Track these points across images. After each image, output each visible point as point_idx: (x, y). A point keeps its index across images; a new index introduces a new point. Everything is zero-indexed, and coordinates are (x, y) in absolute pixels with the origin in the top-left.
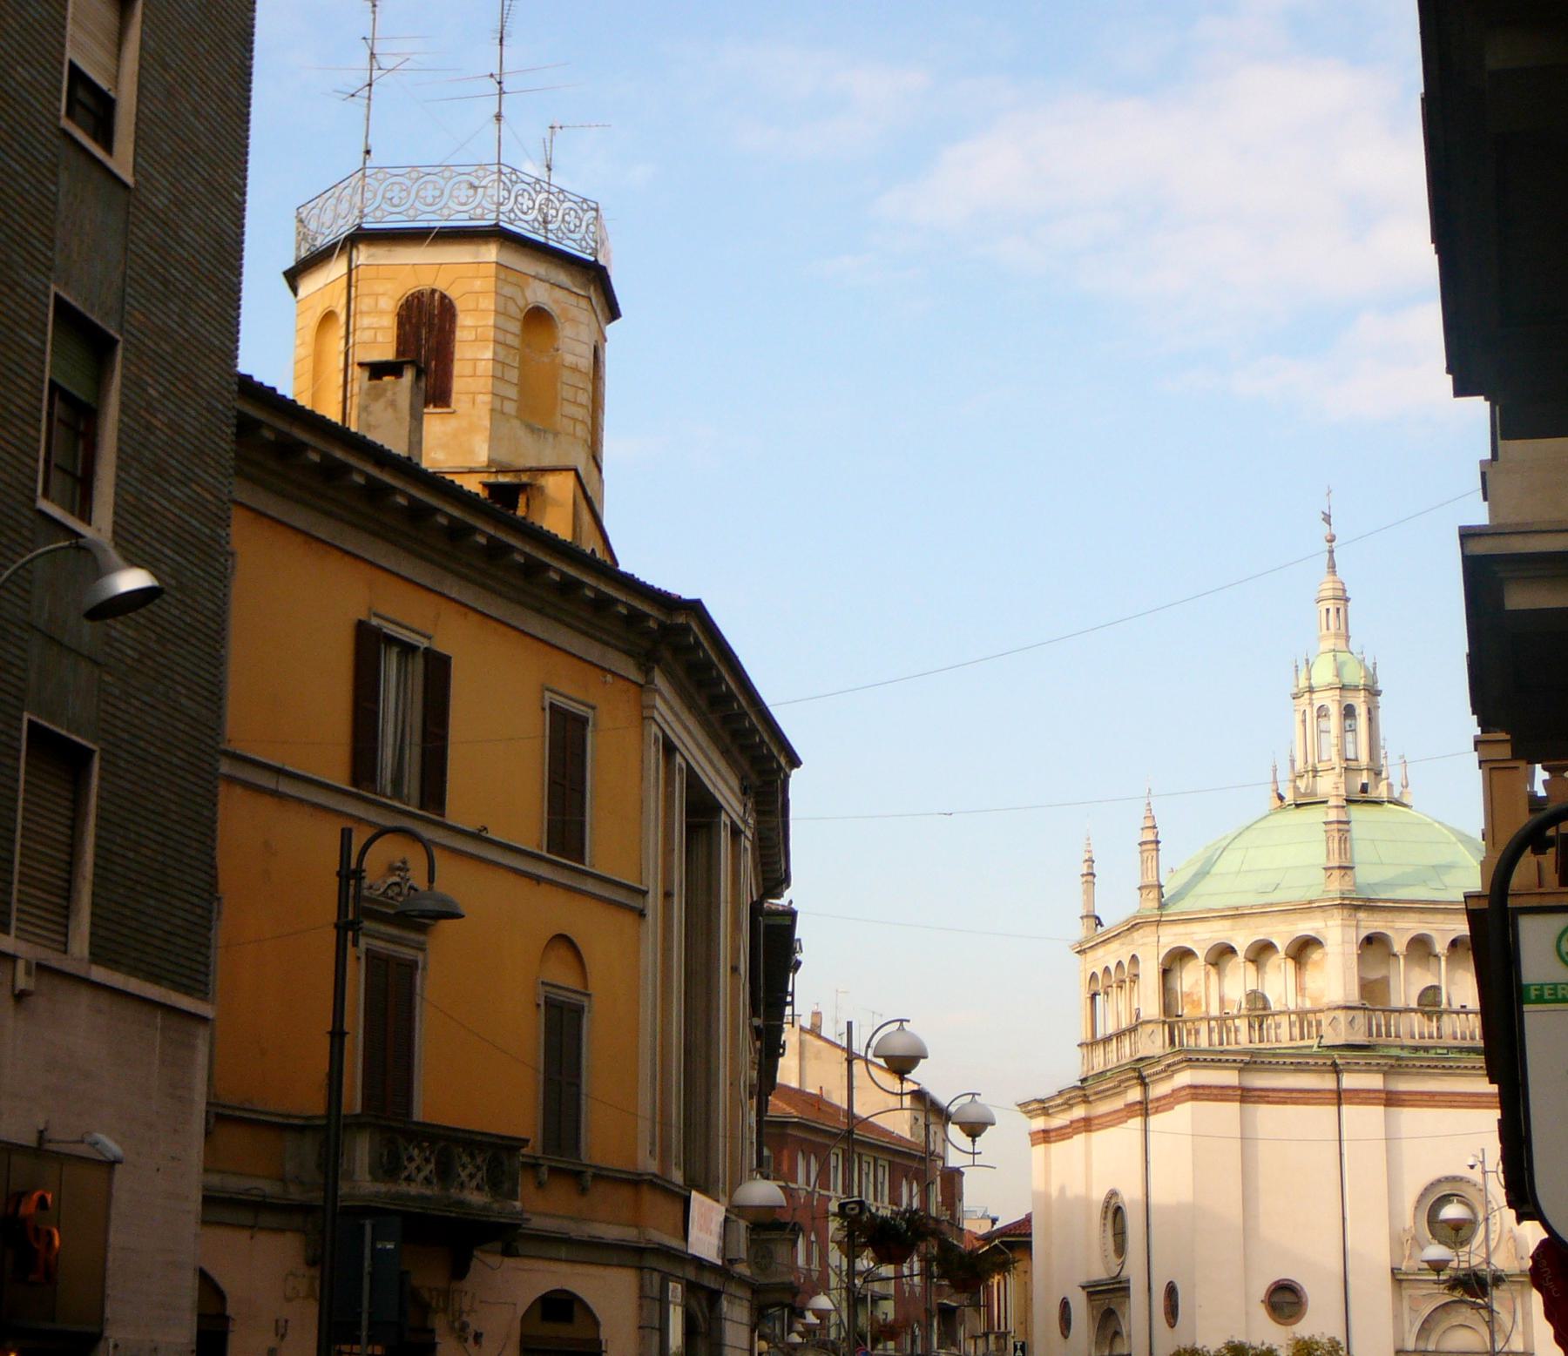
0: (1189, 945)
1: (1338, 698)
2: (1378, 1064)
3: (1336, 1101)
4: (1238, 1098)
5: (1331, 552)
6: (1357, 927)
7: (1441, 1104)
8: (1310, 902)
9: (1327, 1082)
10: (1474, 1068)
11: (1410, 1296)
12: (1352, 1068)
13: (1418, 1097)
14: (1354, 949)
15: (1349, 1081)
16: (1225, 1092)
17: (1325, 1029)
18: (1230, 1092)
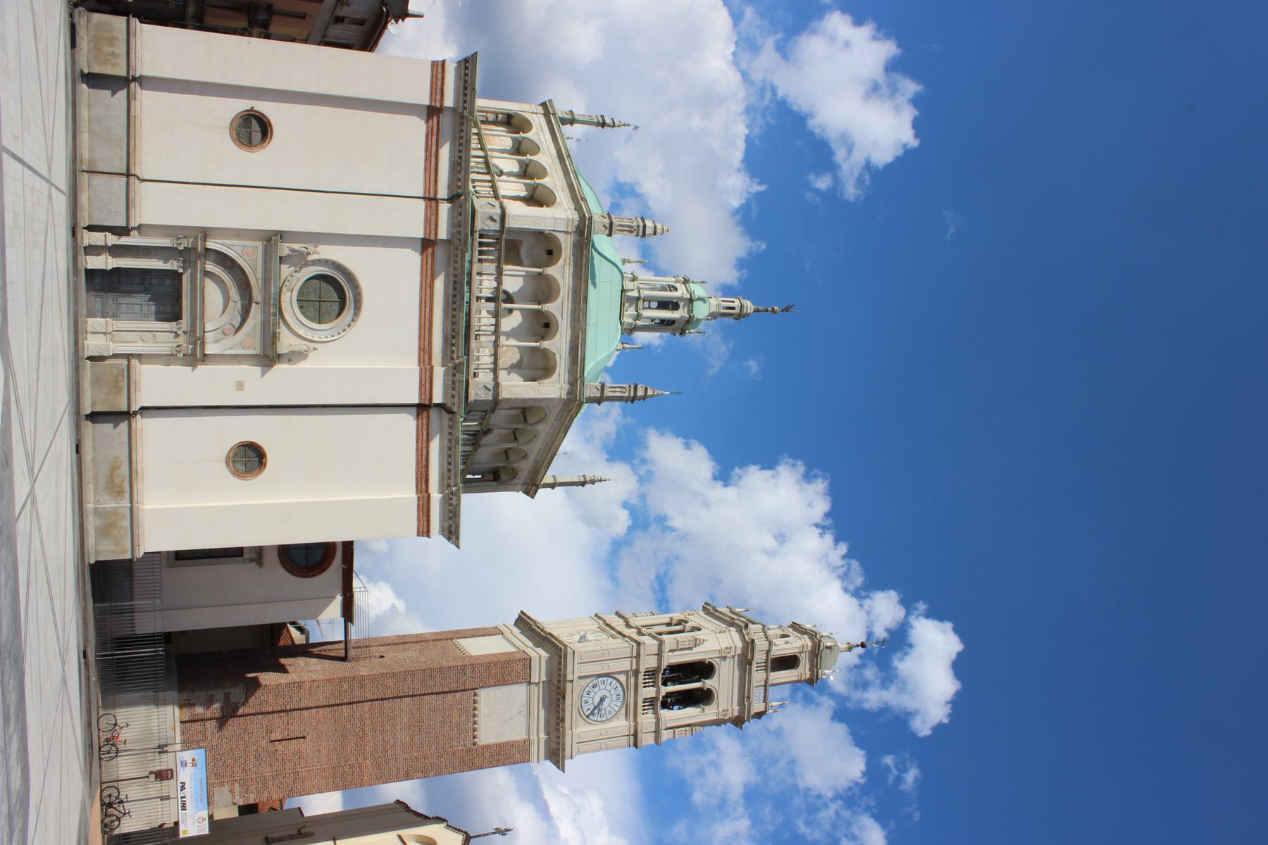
0: (534, 130)
1: (685, 297)
2: (459, 233)
3: (427, 196)
4: (433, 104)
5: (767, 311)
6: (566, 233)
7: (424, 293)
8: (584, 199)
9: (443, 192)
10: (454, 323)
11: (257, 247)
12: (453, 214)
13: (429, 272)
14: (546, 227)
15: (444, 208)
16: (439, 92)
17: (484, 201)
18: (439, 97)
